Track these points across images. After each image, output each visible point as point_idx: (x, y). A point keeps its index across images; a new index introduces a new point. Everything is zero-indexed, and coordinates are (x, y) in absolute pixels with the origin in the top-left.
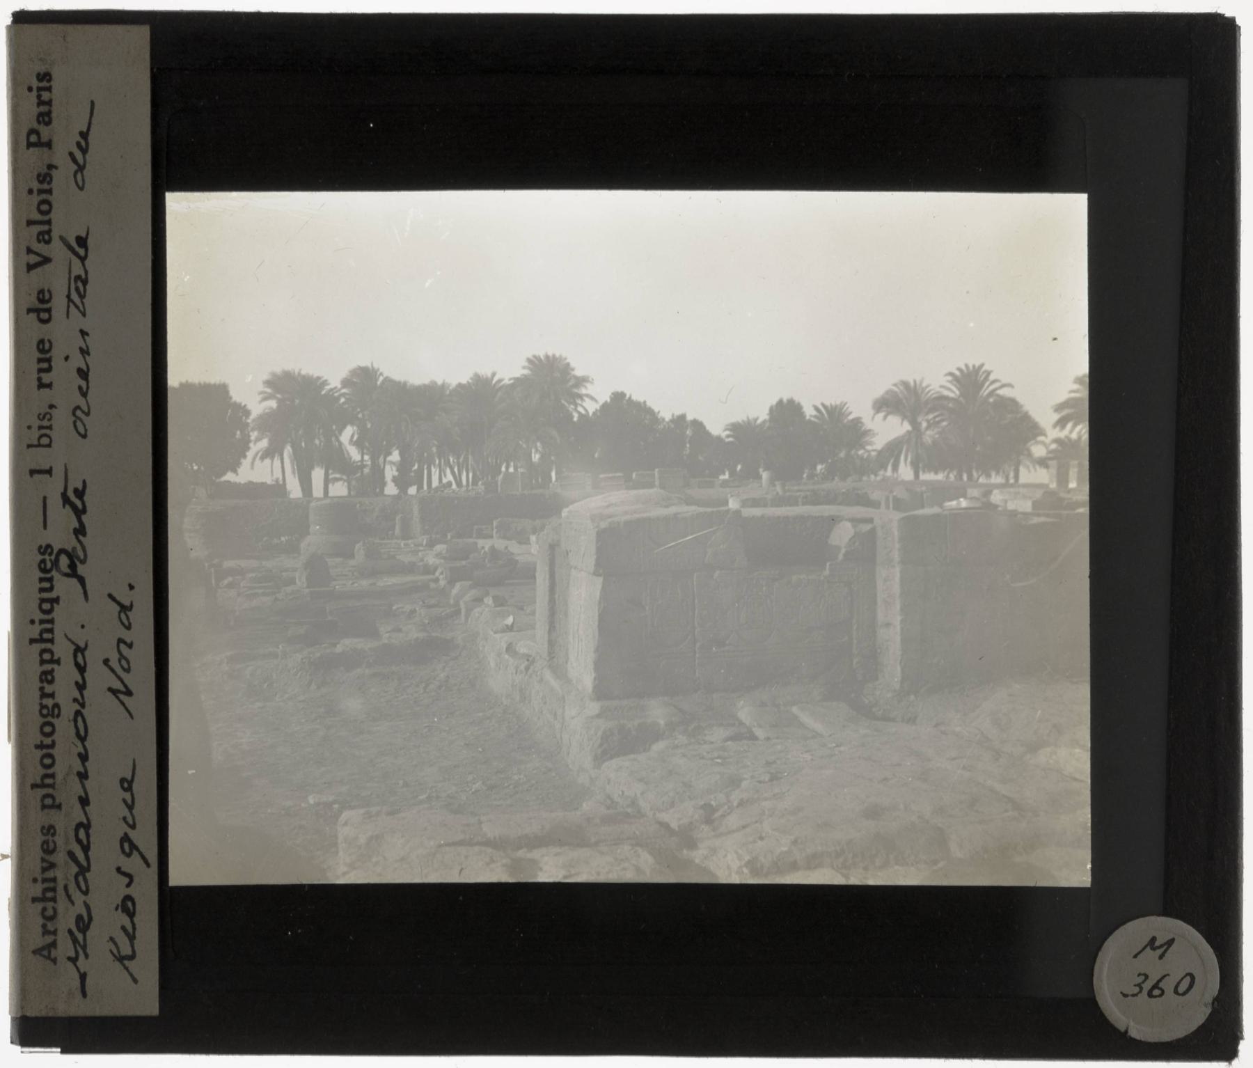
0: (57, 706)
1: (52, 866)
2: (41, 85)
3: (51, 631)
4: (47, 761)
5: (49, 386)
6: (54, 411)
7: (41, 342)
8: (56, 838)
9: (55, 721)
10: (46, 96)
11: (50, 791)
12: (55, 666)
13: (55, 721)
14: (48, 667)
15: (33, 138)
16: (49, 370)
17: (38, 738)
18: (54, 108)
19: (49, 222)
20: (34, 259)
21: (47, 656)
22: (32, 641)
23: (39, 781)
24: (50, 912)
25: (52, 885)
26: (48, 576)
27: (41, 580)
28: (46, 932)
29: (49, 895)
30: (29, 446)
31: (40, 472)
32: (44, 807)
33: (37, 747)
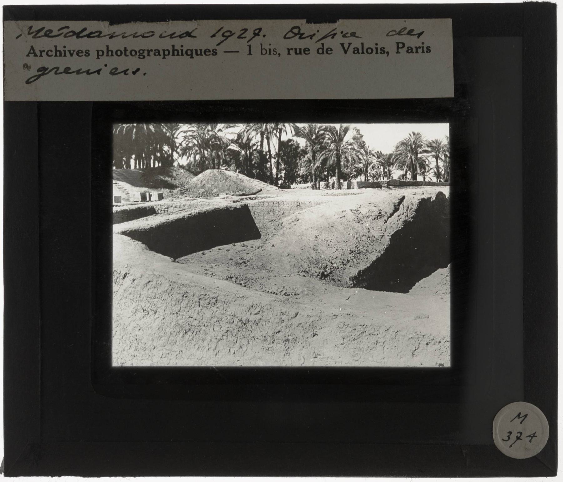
0: (144, 57)
1: (71, 55)
3: (178, 55)
4: (119, 53)
5: (289, 54)
6: (277, 55)
8: (84, 56)
9: (137, 56)
10: (420, 50)
12: (162, 56)
13: (137, 56)
14: (161, 53)
15: (401, 45)
16: (296, 53)
17: (129, 49)
18: (415, 54)
19: (363, 53)
20: (346, 46)
21: (166, 53)
22: (173, 46)
24: (50, 53)
25: (63, 55)
26: (203, 54)
27: (201, 50)
28: (41, 52)
29: (58, 54)
30: (261, 45)
31: (250, 51)
33: (125, 48)
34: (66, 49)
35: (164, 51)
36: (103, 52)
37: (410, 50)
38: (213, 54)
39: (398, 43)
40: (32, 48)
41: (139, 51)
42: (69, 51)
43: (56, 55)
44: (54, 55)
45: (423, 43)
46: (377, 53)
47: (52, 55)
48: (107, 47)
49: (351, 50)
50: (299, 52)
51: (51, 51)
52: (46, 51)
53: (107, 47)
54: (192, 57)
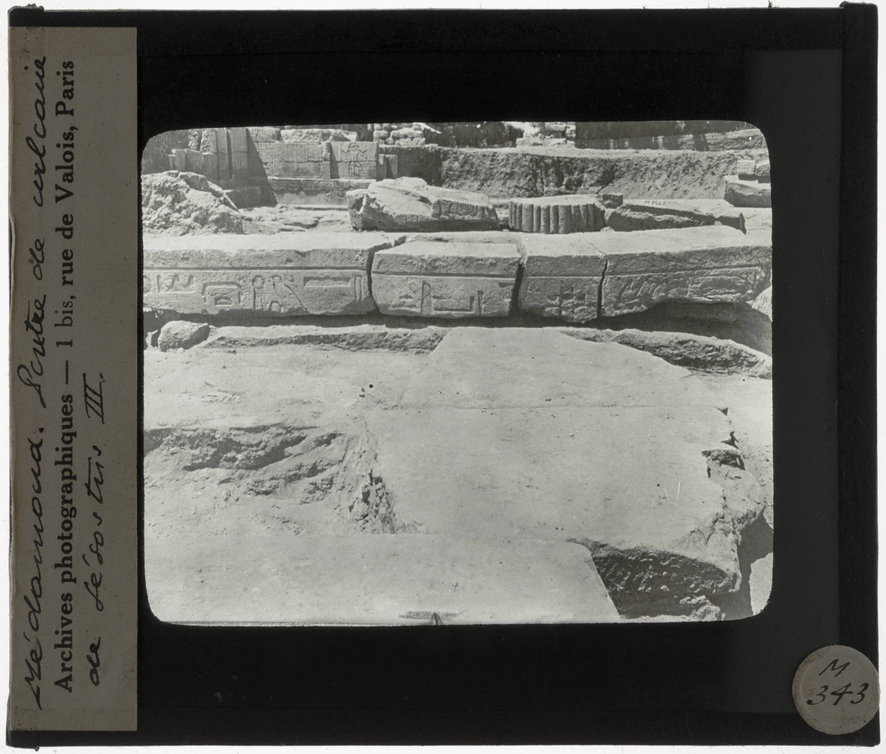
0: (73, 509)
1: (69, 622)
3: (70, 456)
4: (67, 548)
5: (71, 283)
6: (73, 301)
7: (66, 251)
9: (73, 520)
10: (69, 78)
11: (68, 569)
12: (73, 481)
14: (67, 482)
15: (61, 108)
16: (71, 271)
17: (61, 532)
19: (71, 167)
20: (60, 193)
22: (57, 463)
23: (60, 562)
24: (67, 656)
25: (68, 635)
26: (69, 417)
28: (64, 669)
29: (67, 643)
30: (56, 325)
31: (66, 343)
32: (64, 580)
33: (59, 538)
34: (60, 630)
35: (64, 478)
36: (64, 573)
37: (69, 94)
38: (71, 402)
40: (58, 683)
41: (65, 516)
42: (63, 625)
43: (70, 646)
44: (69, 649)
46: (72, 146)
47: (70, 652)
48: (57, 566)
49: (66, 185)
50: (68, 267)
51: (63, 653)
53: (57, 566)
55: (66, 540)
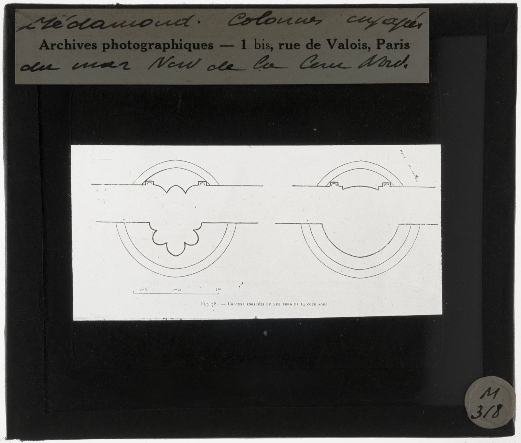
0: (146, 50)
1: (80, 48)
2: (404, 44)
3: (177, 48)
4: (123, 46)
5: (280, 48)
7: (299, 45)
10: (399, 46)
11: (111, 47)
12: (163, 49)
14: (162, 46)
15: (381, 42)
16: (287, 48)
17: (133, 42)
19: (347, 48)
20: (332, 42)
21: (167, 46)
22: (173, 40)
24: (60, 46)
27: (198, 44)
29: (68, 46)
30: (255, 40)
32: (104, 44)
33: (129, 42)
34: (76, 42)
35: (164, 44)
37: (389, 46)
38: (209, 48)
39: (378, 40)
42: (78, 44)
43: (66, 48)
44: (64, 48)
45: (402, 40)
46: (359, 48)
48: (113, 40)
49: (337, 45)
51: (62, 44)
52: (57, 44)
53: (113, 40)
54: (190, 51)
55: (128, 46)
